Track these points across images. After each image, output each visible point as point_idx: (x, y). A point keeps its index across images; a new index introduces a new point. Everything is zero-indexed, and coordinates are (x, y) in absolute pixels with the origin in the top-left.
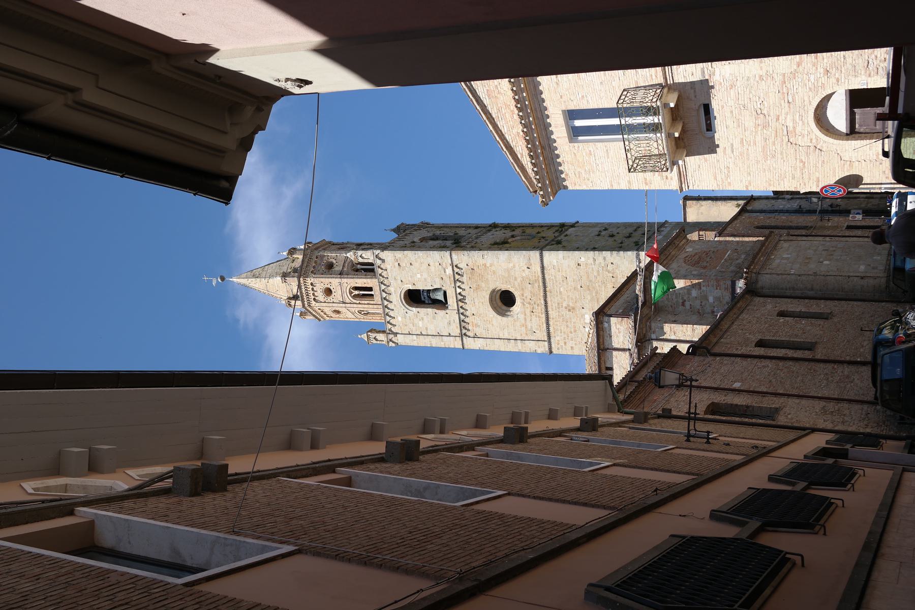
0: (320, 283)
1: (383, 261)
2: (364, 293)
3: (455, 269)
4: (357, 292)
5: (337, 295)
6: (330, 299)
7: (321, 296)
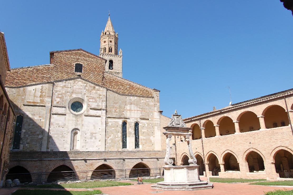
0: (113, 42)
1: (120, 57)
2: (110, 50)
3: (118, 73)
4: (111, 48)
5: (110, 43)
6: (109, 42)
7: (110, 39)
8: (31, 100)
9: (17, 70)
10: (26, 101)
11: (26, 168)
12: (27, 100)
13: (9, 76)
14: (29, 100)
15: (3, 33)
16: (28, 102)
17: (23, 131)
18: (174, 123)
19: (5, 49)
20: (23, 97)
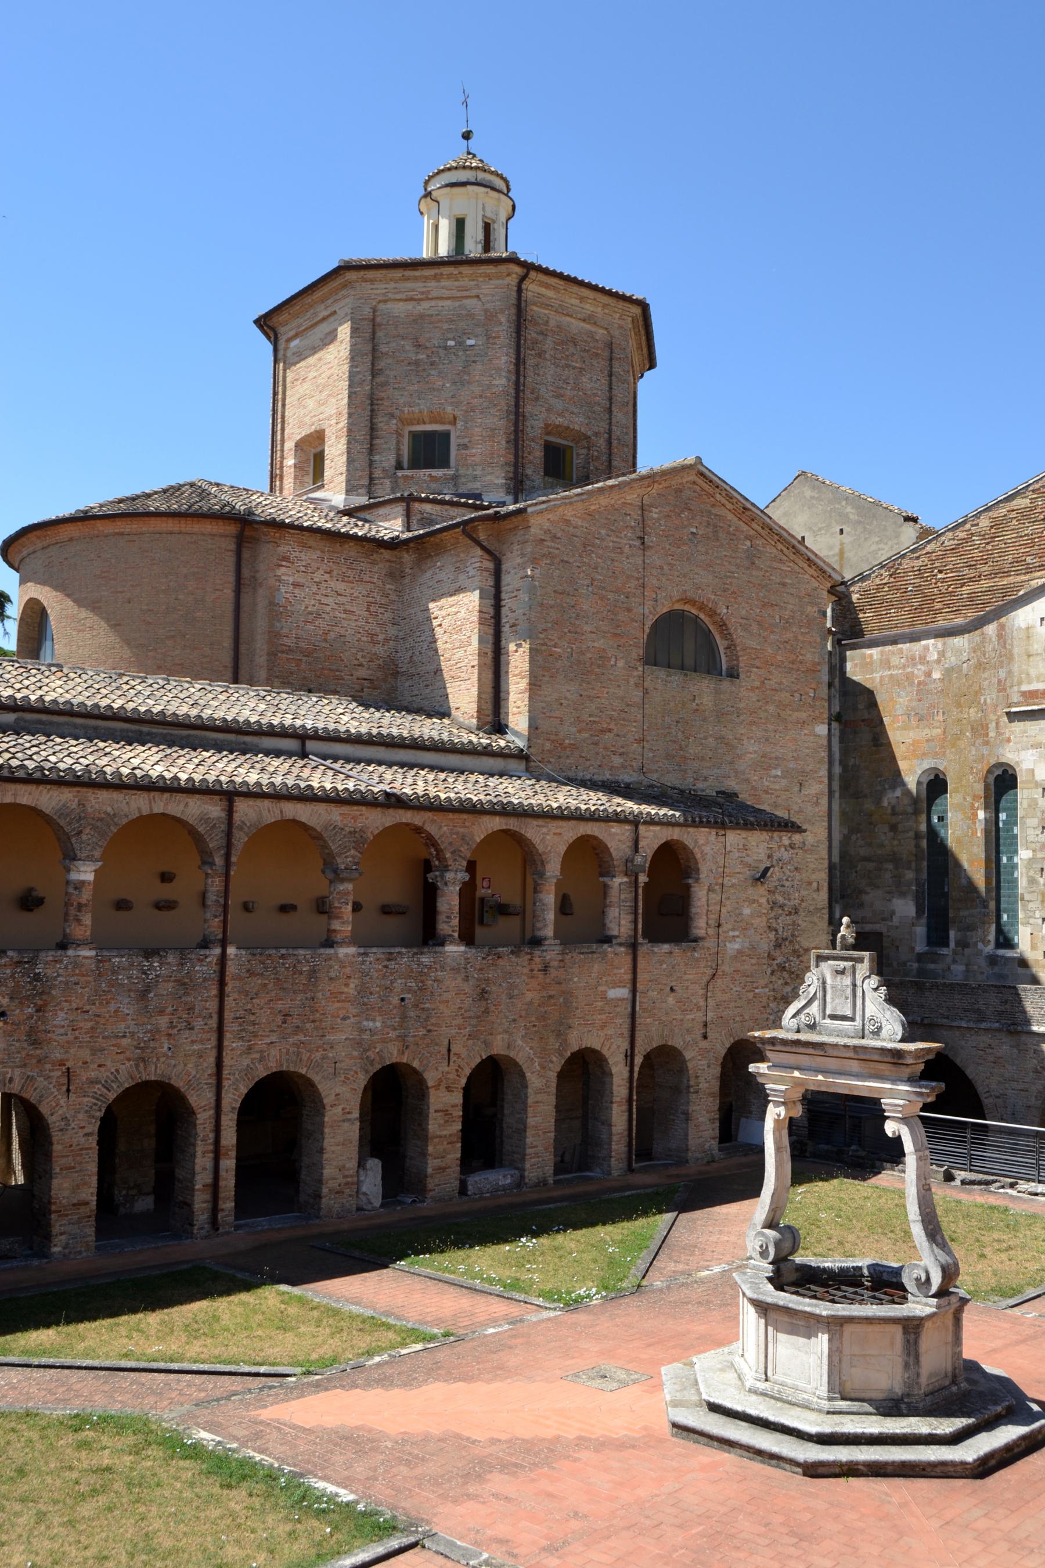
8: (1038, 681)
9: (968, 526)
10: (1015, 689)
11: (958, 1061)
12: (1020, 683)
13: (940, 572)
14: (1029, 683)
15: (691, 460)
16: (1024, 694)
17: (1024, 854)
18: (815, 1009)
19: (745, 510)
20: (1002, 674)
